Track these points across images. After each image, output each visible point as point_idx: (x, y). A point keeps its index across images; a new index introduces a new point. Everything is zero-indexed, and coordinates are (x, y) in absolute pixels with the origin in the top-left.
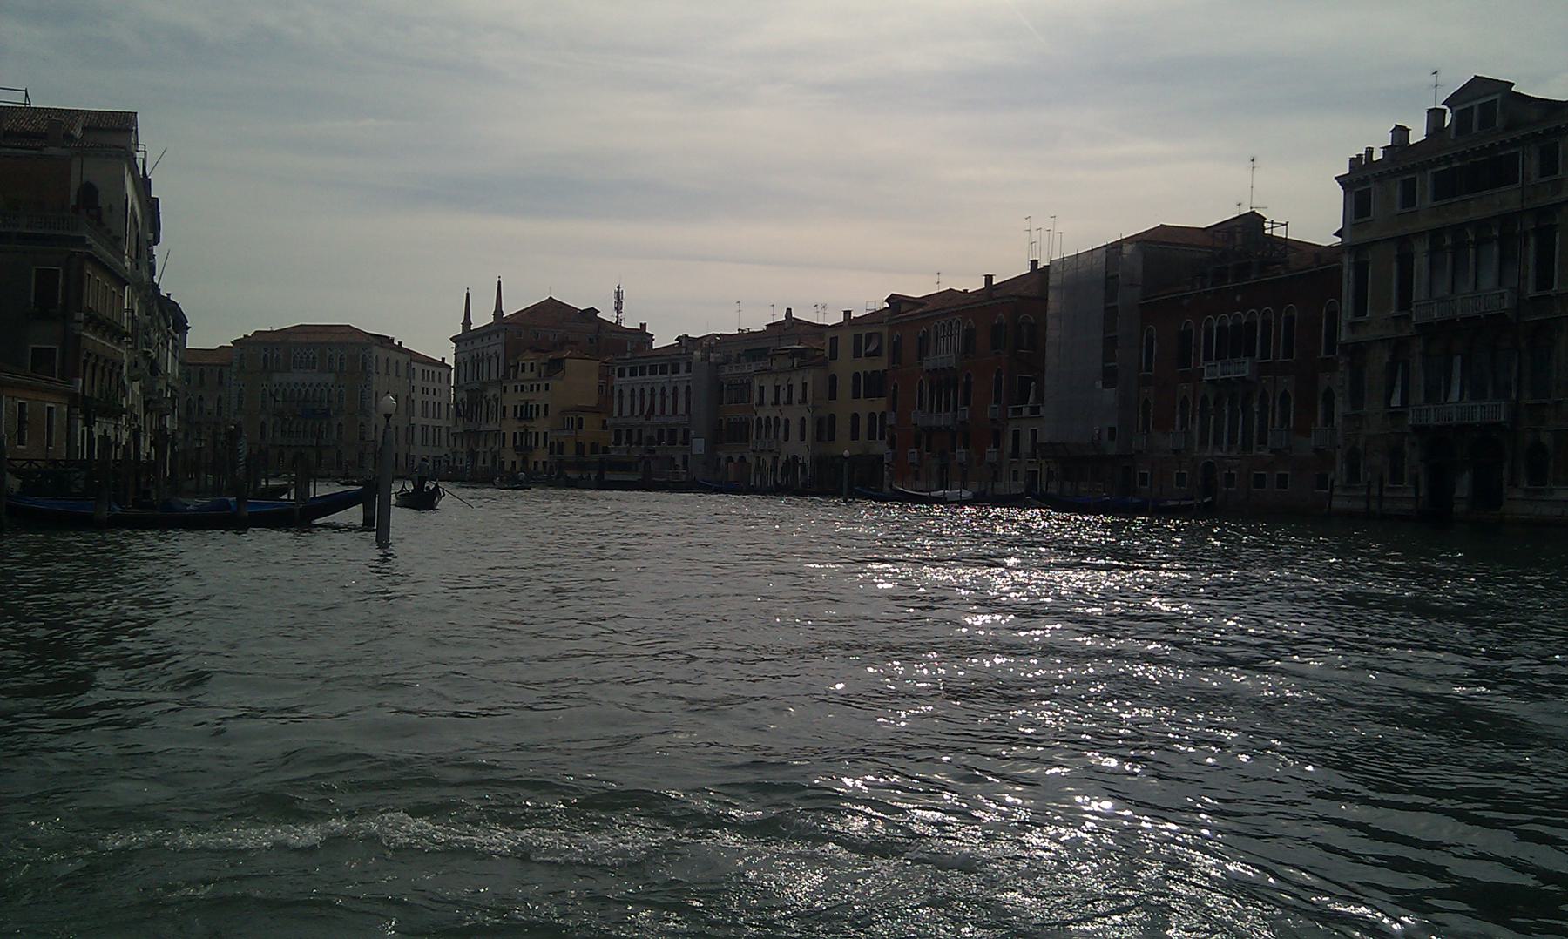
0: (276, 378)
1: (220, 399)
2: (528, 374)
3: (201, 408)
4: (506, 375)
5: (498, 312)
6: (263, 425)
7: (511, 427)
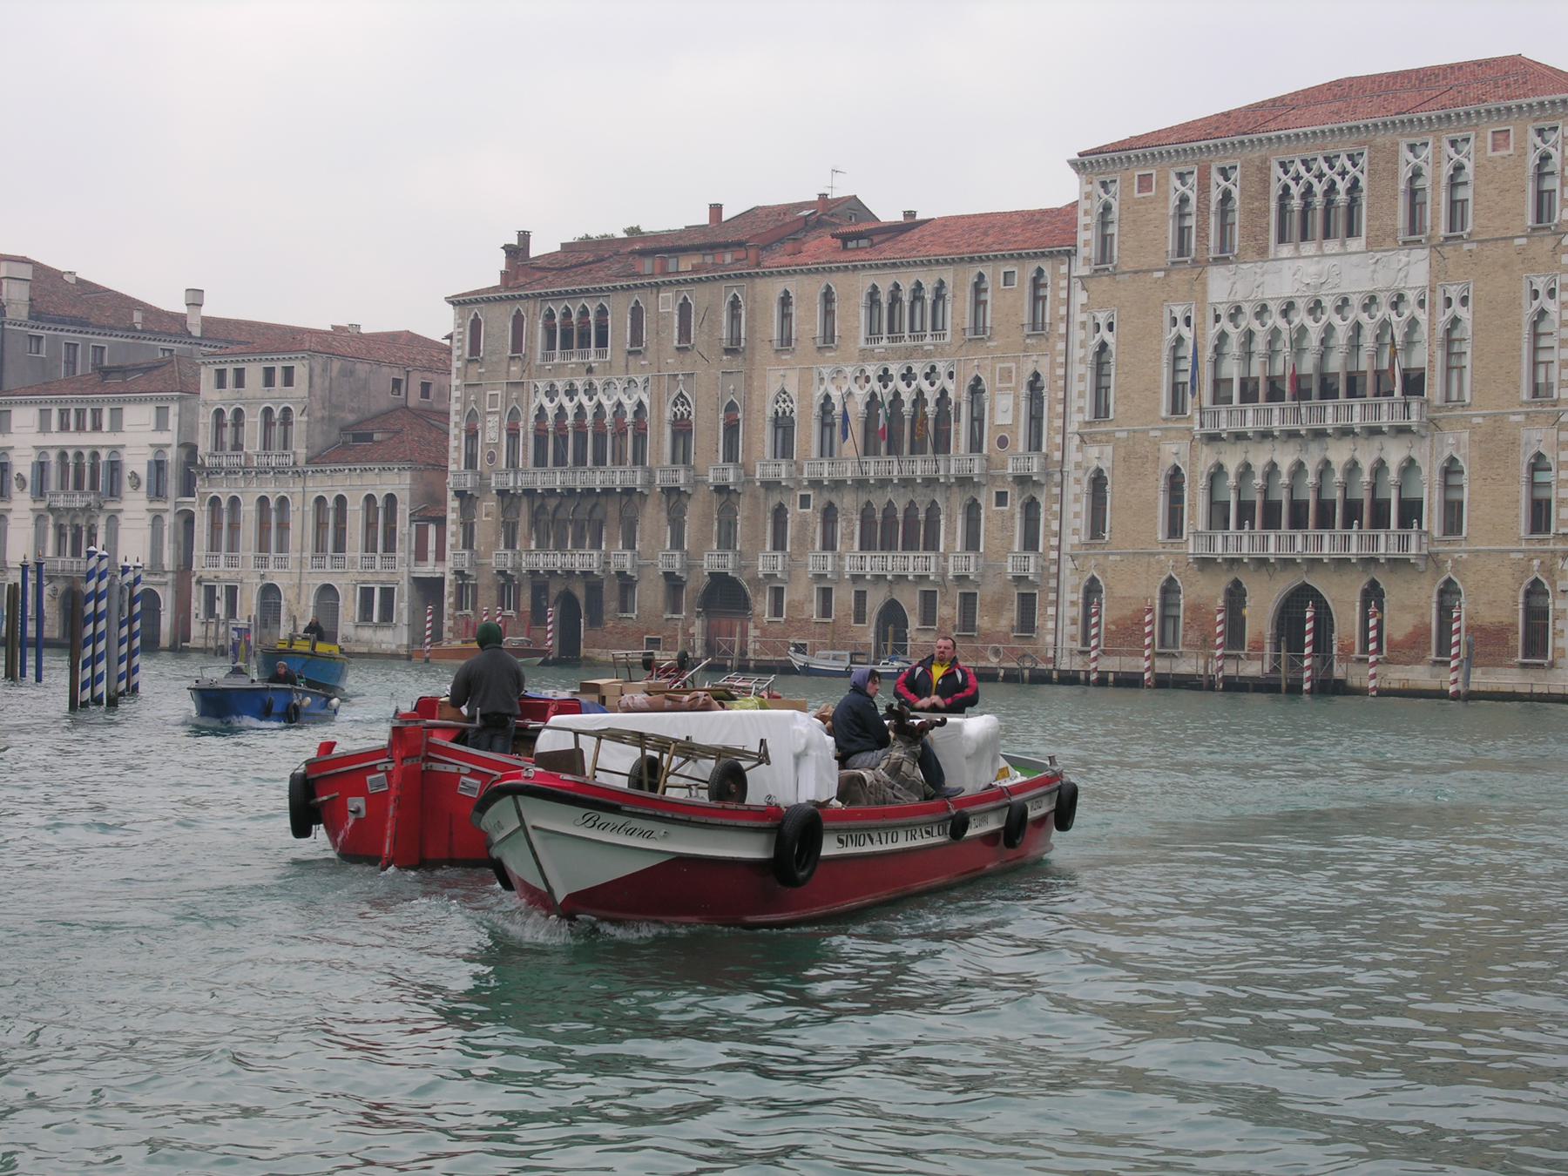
0: (1221, 286)
3: (977, 420)
6: (1175, 480)
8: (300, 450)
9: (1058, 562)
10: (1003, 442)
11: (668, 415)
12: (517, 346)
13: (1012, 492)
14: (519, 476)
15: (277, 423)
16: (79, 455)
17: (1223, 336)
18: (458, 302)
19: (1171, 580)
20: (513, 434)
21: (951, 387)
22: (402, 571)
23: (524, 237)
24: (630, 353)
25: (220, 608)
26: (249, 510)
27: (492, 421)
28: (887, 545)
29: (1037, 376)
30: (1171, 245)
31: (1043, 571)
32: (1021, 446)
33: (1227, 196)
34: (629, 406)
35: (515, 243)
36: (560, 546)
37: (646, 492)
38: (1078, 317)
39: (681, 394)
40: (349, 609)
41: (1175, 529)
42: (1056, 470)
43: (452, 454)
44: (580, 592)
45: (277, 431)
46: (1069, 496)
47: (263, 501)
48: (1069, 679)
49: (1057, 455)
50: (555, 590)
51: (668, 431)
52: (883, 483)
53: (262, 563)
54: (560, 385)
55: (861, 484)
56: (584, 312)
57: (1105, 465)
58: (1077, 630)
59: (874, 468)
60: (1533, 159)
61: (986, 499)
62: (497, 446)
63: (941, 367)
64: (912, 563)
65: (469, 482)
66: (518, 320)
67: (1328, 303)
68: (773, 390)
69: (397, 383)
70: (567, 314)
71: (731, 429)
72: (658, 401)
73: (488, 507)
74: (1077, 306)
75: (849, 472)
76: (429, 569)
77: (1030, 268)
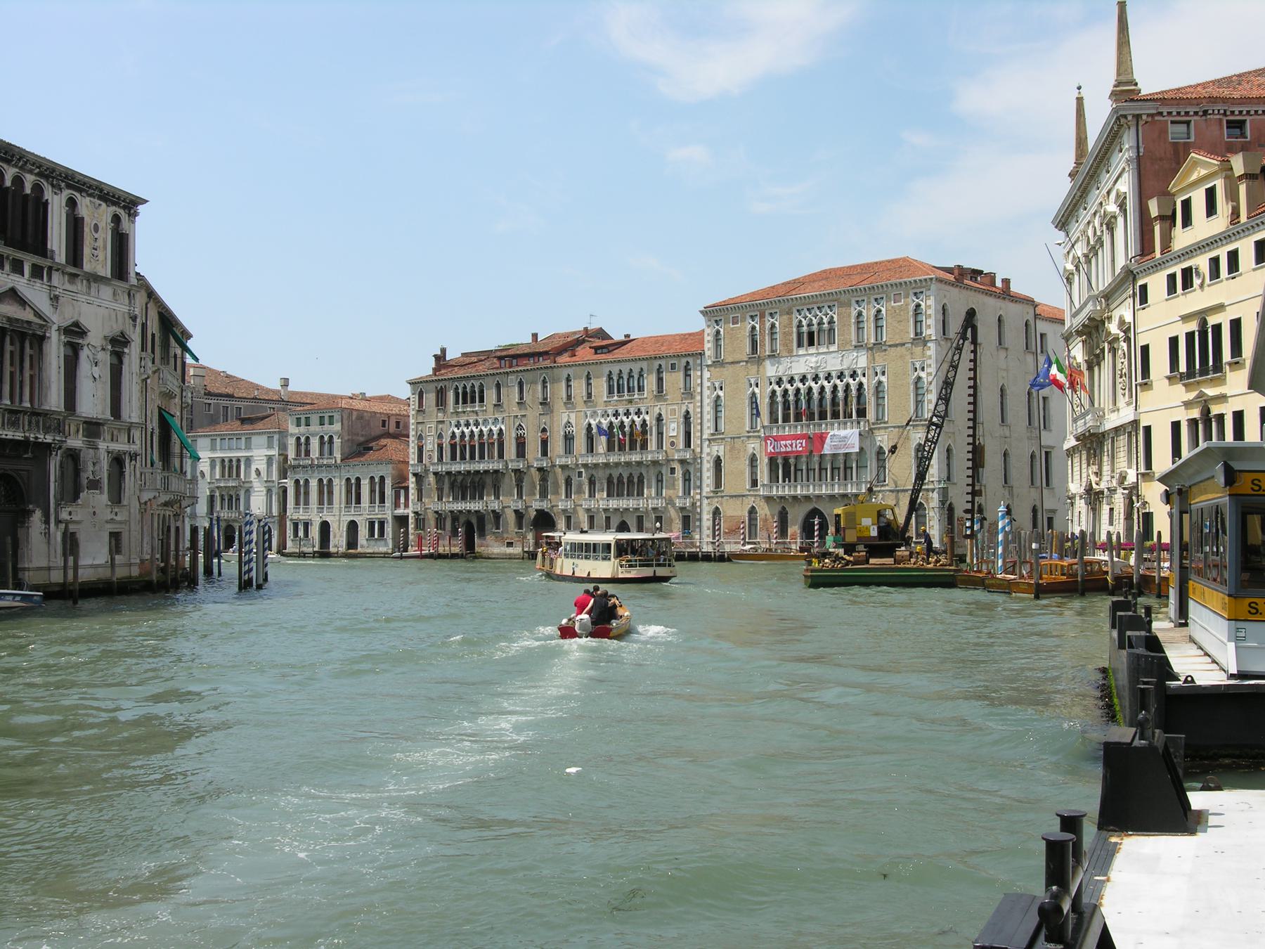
0: (771, 370)
1: (687, 416)
2: (1204, 227)
3: (660, 434)
4: (1145, 246)
5: (1125, 92)
6: (753, 459)
7: (1165, 404)
8: (338, 455)
9: (700, 500)
10: (672, 444)
11: (514, 435)
13: (677, 466)
15: (326, 443)
16: (231, 461)
17: (774, 392)
18: (413, 383)
19: (753, 507)
20: (440, 447)
21: (647, 418)
22: (388, 513)
23: (443, 351)
25: (301, 534)
26: (314, 484)
27: (430, 439)
28: (620, 495)
29: (688, 412)
30: (748, 349)
31: (693, 504)
32: (681, 446)
33: (773, 326)
34: (495, 429)
35: (439, 353)
36: (464, 498)
38: (707, 384)
40: (363, 532)
41: (754, 483)
42: (697, 459)
43: (411, 456)
44: (474, 521)
45: (326, 446)
46: (705, 469)
47: (320, 481)
48: (707, 558)
49: (698, 450)
50: (462, 519)
52: (617, 464)
53: (320, 510)
55: (607, 465)
56: (473, 386)
57: (721, 454)
58: (710, 532)
59: (613, 459)
60: (912, 306)
61: (665, 471)
63: (643, 410)
64: (631, 503)
67: (821, 375)
68: (565, 421)
69: (384, 422)
70: (465, 387)
71: (544, 443)
72: (509, 429)
73: (432, 478)
74: (704, 378)
75: (602, 460)
76: (401, 511)
77: (684, 361)
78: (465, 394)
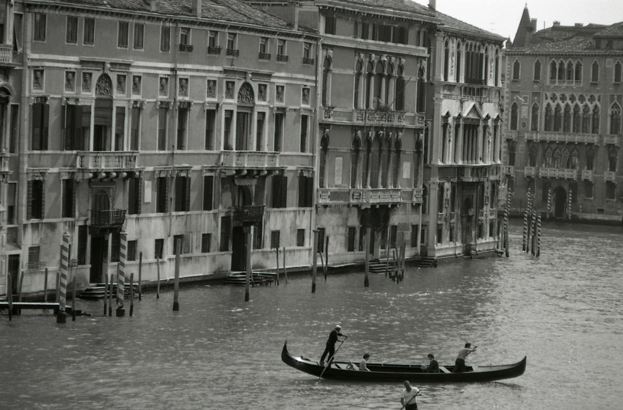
11: (609, 112)
12: (537, 76)
14: (539, 134)
24: (592, 84)
34: (591, 106)
37: (599, 145)
39: (616, 104)
44: (566, 187)
50: (555, 185)
51: (609, 119)
54: (558, 95)
62: (528, 119)
65: (513, 136)
66: (538, 66)
70: (562, 64)
78: (561, 70)
